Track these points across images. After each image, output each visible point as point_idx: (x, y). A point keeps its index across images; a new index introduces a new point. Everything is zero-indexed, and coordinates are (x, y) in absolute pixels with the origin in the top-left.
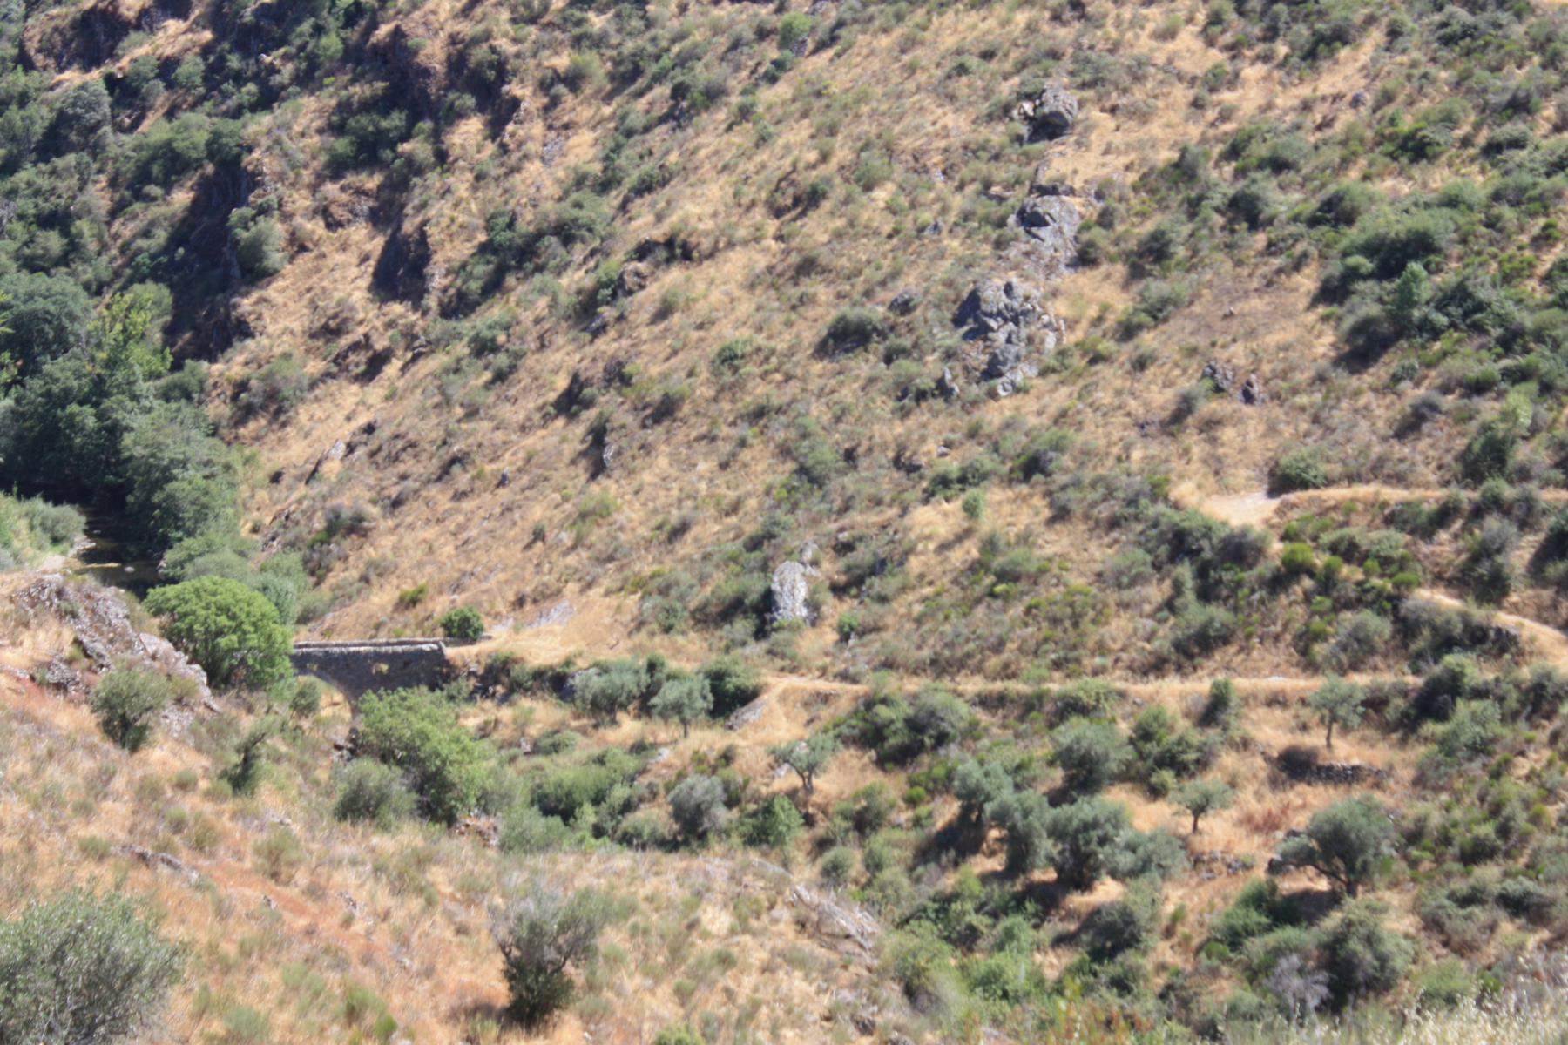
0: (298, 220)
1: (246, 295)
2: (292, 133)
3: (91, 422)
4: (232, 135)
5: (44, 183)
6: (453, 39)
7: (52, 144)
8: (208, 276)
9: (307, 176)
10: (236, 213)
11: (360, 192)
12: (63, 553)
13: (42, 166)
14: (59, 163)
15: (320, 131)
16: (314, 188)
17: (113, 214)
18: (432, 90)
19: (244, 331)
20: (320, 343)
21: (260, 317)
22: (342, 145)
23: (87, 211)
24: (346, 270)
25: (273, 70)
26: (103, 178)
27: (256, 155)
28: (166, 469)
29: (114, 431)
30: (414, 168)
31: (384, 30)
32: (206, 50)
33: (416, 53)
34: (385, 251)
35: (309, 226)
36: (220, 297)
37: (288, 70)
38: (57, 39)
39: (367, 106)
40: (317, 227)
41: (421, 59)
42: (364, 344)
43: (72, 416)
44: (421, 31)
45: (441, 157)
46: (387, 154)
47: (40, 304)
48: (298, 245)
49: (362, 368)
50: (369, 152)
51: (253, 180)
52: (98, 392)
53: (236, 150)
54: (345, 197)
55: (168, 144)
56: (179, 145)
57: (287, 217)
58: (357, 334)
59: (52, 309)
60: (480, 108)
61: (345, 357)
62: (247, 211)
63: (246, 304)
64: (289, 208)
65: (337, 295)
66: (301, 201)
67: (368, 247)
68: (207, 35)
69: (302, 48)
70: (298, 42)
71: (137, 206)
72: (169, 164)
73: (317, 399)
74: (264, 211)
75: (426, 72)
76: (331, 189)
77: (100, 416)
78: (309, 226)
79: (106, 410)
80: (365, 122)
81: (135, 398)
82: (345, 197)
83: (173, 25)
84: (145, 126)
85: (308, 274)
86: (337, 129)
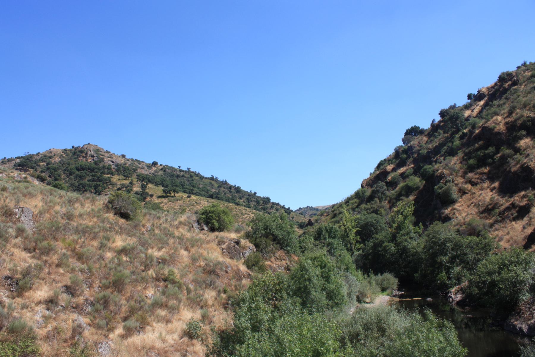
0: (460, 185)
1: (447, 209)
2: (450, 166)
3: (393, 249)
4: (430, 168)
5: (369, 207)
6: (506, 123)
7: (371, 199)
8: (432, 204)
9: (460, 174)
10: (436, 187)
11: (482, 174)
12: (388, 295)
13: (368, 203)
14: (373, 202)
15: (461, 163)
16: (463, 177)
17: (390, 208)
18: (503, 137)
19: (447, 219)
20: (486, 214)
21: (454, 214)
22: (471, 161)
23: (382, 207)
24: (487, 194)
25: (437, 159)
26: (386, 201)
27: (440, 171)
28: (444, 244)
29: (403, 251)
30: (504, 159)
31: (477, 131)
32: (413, 168)
33: (494, 130)
34: (501, 185)
35: (466, 186)
36: (436, 212)
37: (442, 158)
38: (371, 182)
39: (478, 150)
40: (469, 186)
41: (496, 130)
42: (513, 205)
43: (385, 247)
44: (493, 125)
45: (517, 151)
46: (490, 160)
47: (370, 220)
48: (463, 192)
49: (516, 214)
50: (482, 162)
51: (442, 176)
52: (393, 238)
53: (432, 172)
54: (476, 176)
55: (407, 185)
56: (410, 184)
57: (457, 185)
58: (507, 205)
59: (374, 222)
60: (528, 135)
61: (503, 214)
62: (441, 184)
63: (447, 211)
64: (456, 182)
65: (488, 199)
66: (460, 180)
67: (493, 185)
68: (412, 166)
69: (445, 152)
70: (444, 151)
71: (400, 202)
72: (408, 191)
73: (496, 230)
74: (446, 182)
75: (499, 133)
76: (470, 175)
77: (397, 245)
78: (466, 186)
79: (400, 243)
80: (480, 153)
81: (411, 238)
82: (476, 176)
83: (402, 169)
84: (397, 189)
85: (470, 200)
86: (469, 158)
